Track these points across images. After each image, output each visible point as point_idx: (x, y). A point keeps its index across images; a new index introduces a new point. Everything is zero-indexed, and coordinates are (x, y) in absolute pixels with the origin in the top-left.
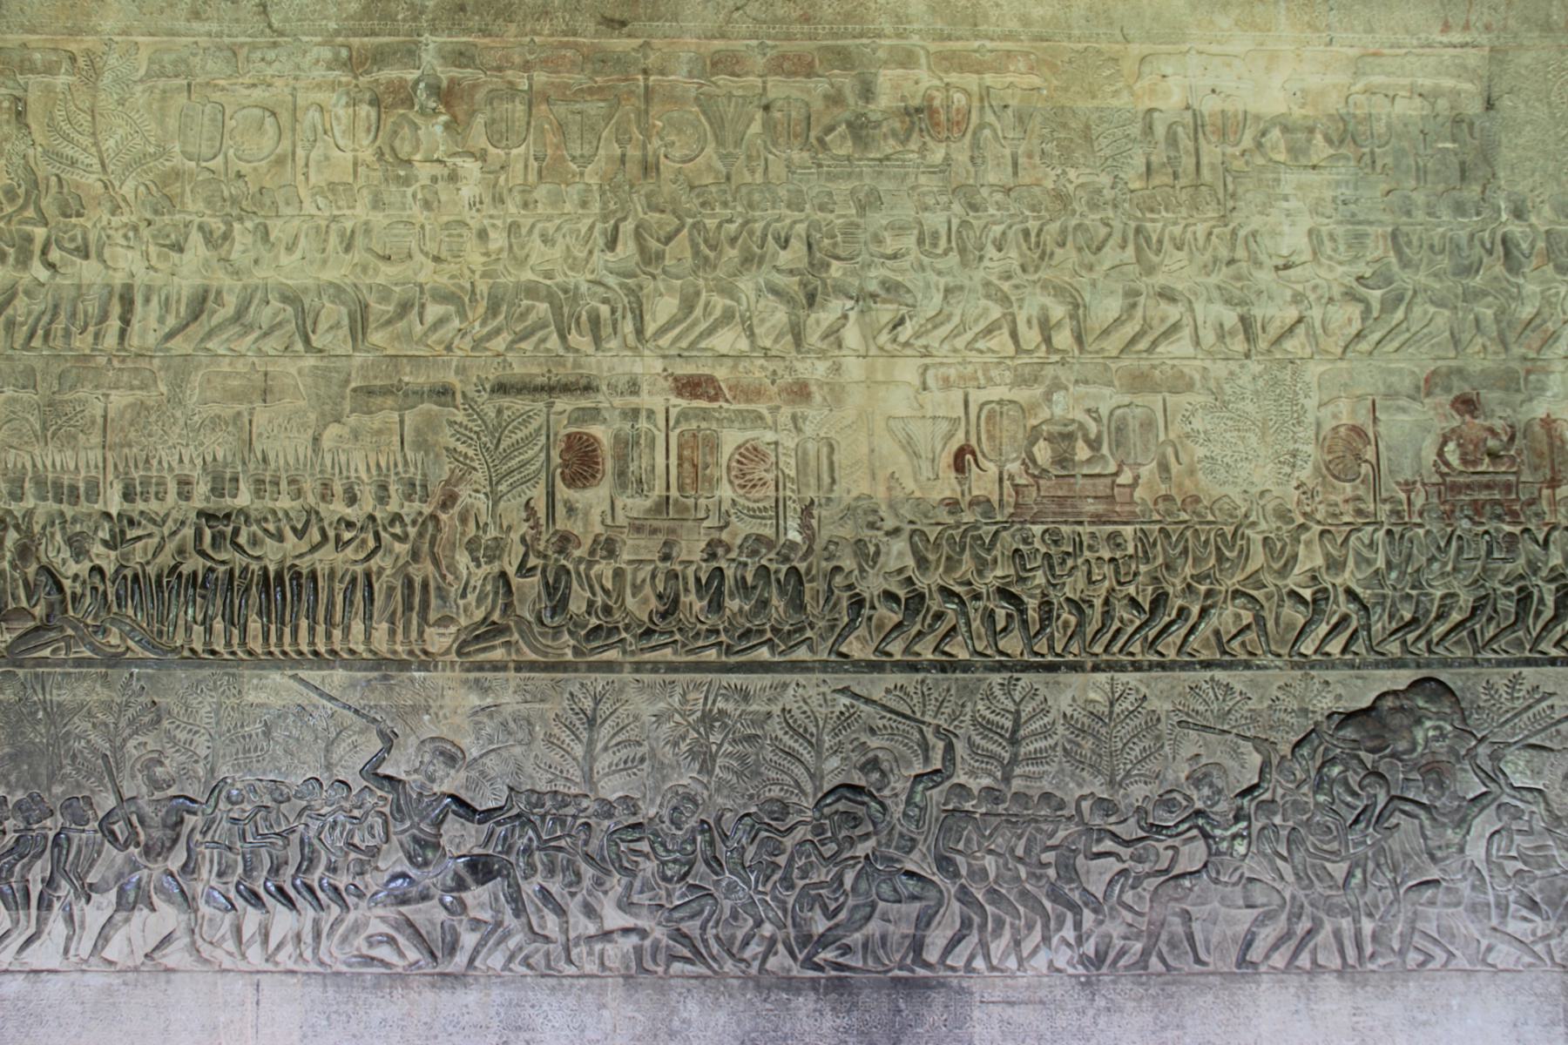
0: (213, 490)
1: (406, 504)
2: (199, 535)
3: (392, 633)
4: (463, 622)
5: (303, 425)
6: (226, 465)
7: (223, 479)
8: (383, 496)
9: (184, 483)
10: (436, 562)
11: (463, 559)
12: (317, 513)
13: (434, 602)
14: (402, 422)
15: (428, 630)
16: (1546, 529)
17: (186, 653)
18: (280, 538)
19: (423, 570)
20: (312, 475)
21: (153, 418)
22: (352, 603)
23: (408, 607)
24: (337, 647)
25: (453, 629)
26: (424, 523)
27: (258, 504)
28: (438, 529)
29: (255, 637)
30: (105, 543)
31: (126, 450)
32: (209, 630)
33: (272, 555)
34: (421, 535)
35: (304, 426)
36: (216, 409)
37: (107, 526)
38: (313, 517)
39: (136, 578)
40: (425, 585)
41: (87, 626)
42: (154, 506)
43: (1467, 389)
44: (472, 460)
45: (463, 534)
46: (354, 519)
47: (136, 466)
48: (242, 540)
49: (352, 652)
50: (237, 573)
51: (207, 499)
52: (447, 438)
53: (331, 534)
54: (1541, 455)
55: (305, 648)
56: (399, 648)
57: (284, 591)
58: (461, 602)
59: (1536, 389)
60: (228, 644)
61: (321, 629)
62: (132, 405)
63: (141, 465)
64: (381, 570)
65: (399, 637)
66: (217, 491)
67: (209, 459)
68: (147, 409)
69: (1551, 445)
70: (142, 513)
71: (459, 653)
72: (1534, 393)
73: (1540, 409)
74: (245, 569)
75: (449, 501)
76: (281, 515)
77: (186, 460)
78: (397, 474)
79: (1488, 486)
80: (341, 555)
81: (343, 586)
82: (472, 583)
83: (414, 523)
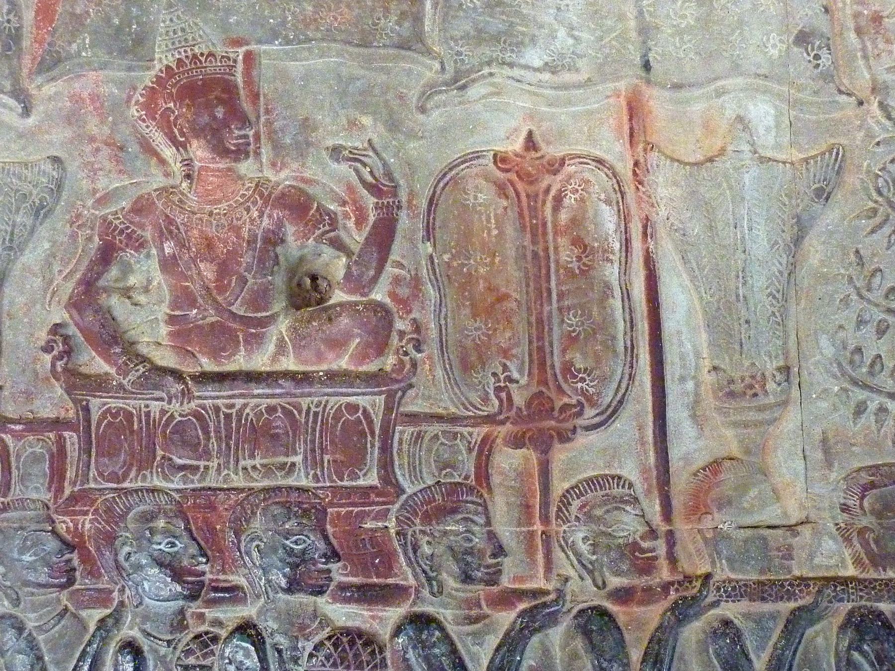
16: (506, 618)
43: (208, 38)
54: (491, 306)
59: (480, 37)
69: (538, 264)
72: (471, 55)
73: (499, 117)
79: (261, 435)
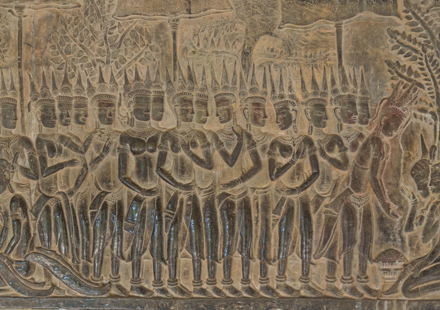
0: (137, 111)
1: (345, 125)
2: (123, 160)
3: (332, 268)
4: (409, 256)
5: (231, 37)
6: (149, 85)
7: (148, 99)
8: (319, 121)
9: (106, 104)
10: (378, 190)
11: (408, 187)
12: (249, 136)
13: (376, 234)
14: (339, 33)
15: (370, 265)
17: (114, 291)
18: (208, 164)
19: (364, 199)
20: (242, 94)
21: (70, 33)
22: (288, 234)
23: (349, 241)
24: (273, 284)
25: (399, 265)
26: (365, 146)
27: (185, 127)
28: (380, 153)
29: (186, 273)
30: (25, 171)
31: (43, 69)
32: (137, 267)
33: (201, 183)
34: (362, 160)
35: (232, 39)
36: (137, 22)
37: (26, 152)
38: (245, 141)
39: (59, 209)
40: (367, 216)
41: (11, 262)
42: (74, 129)
44: (417, 75)
45: (408, 158)
46: (290, 143)
47: (55, 87)
48: (169, 166)
49: (289, 289)
50: (164, 204)
51: (131, 122)
52: (389, 50)
53: (264, 159)
55: (238, 286)
56: (340, 285)
57: (219, 223)
58: (406, 235)
60: (158, 281)
61: (255, 264)
62: (47, 19)
63: (59, 86)
64: (319, 199)
65: (340, 273)
66: (141, 113)
67: (131, 77)
68: (63, 22)
70: (62, 138)
71: (405, 290)
74: (173, 201)
75: (392, 122)
76: (209, 139)
77: (107, 79)
78: (335, 91)
80: (274, 183)
81: (279, 217)
82: (418, 213)
83: (354, 146)
